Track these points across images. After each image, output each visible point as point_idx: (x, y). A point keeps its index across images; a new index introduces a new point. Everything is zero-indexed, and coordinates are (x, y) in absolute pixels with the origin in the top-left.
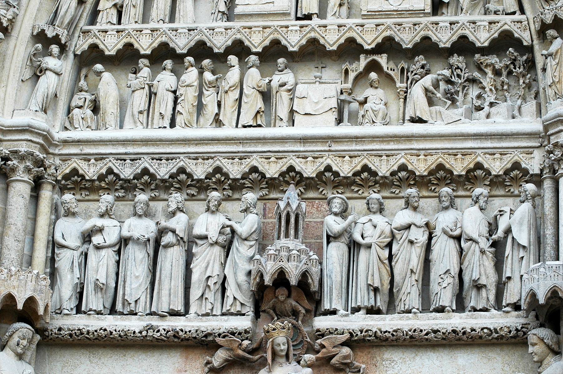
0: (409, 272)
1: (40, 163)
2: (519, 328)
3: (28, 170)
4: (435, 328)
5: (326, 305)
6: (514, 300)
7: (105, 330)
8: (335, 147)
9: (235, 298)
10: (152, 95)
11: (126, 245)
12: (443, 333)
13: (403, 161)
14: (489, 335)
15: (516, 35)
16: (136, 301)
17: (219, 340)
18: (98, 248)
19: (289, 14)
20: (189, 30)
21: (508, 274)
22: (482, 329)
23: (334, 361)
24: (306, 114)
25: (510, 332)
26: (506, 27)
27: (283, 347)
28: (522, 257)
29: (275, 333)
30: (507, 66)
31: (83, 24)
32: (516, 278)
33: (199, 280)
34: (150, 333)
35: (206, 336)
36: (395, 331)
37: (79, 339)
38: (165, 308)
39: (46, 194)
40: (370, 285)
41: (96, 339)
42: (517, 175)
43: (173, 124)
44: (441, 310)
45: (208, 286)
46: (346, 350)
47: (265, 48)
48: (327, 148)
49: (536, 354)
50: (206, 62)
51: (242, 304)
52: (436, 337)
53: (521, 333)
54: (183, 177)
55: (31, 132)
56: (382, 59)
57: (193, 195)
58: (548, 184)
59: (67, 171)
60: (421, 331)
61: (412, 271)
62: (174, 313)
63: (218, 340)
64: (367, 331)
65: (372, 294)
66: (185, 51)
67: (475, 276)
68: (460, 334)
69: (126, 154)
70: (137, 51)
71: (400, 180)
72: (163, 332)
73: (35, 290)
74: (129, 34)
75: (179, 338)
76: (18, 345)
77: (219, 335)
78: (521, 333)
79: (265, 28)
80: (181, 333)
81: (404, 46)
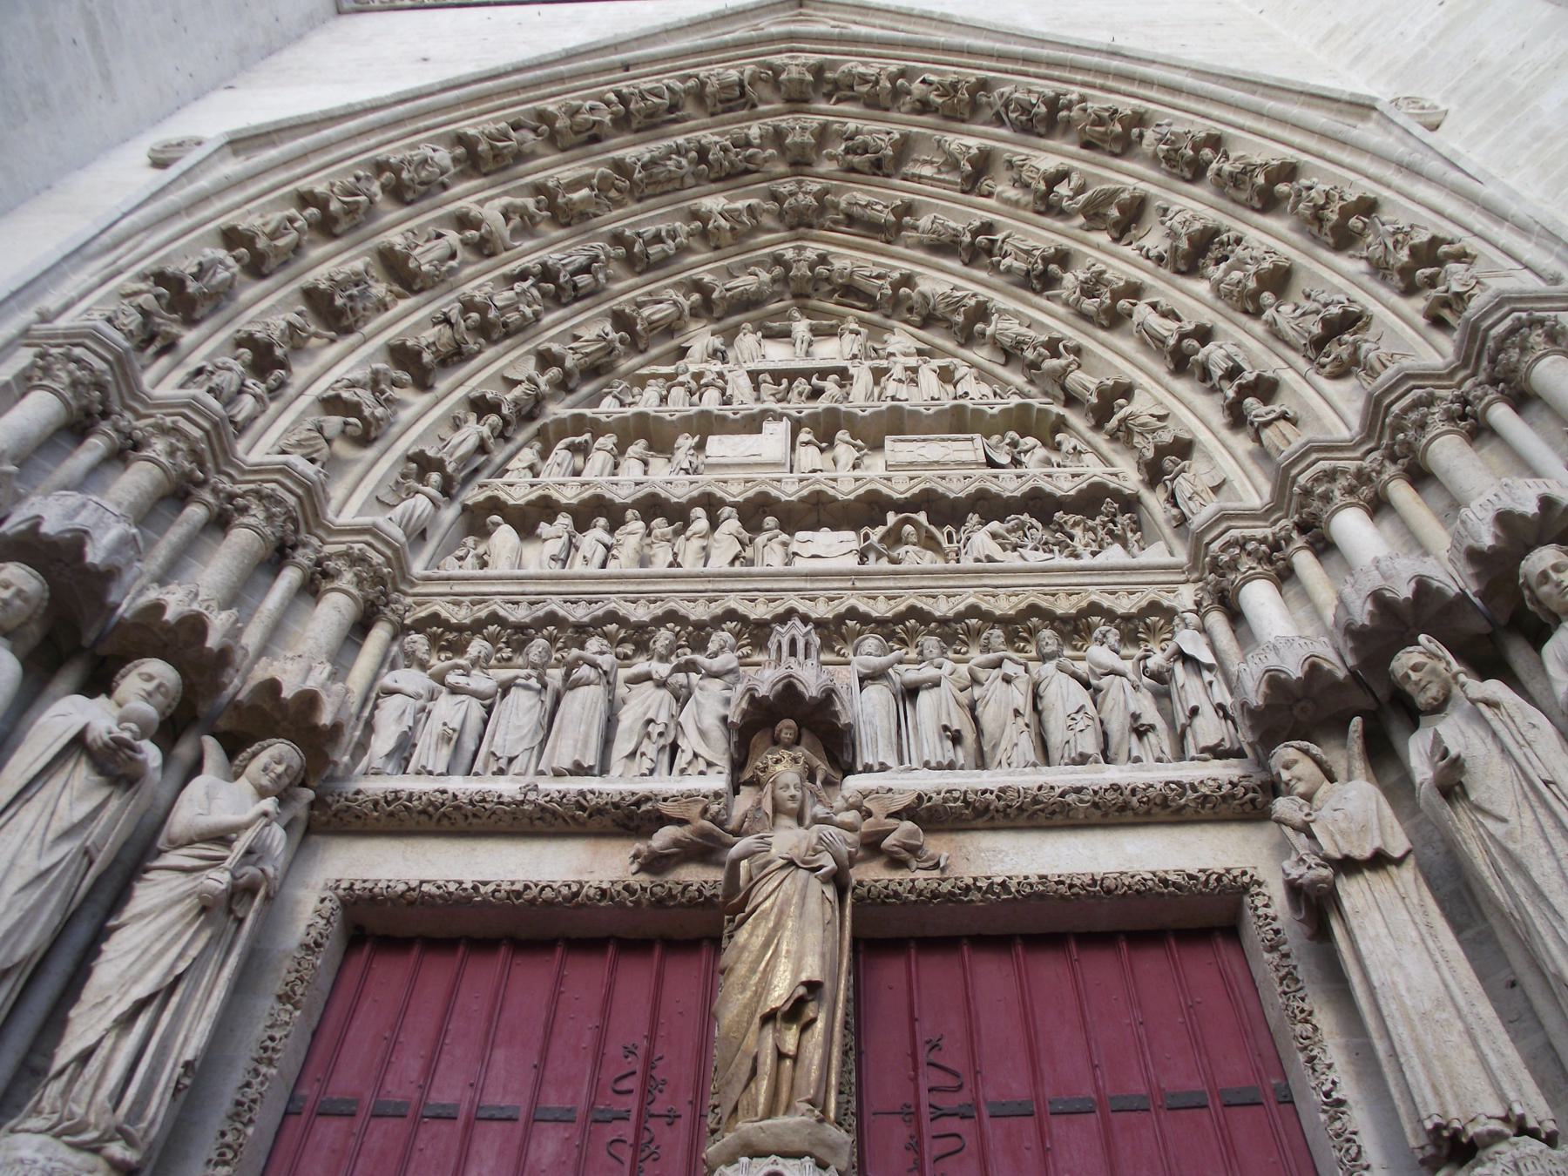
0: (1011, 713)
1: (379, 579)
2: (1235, 780)
3: (360, 582)
4: (1079, 785)
5: (869, 759)
6: (1211, 741)
7: (444, 792)
8: (858, 584)
9: (696, 755)
10: (571, 546)
11: (504, 695)
12: (1095, 792)
13: (972, 600)
14: (1181, 796)
15: (1112, 485)
16: (511, 760)
17: (668, 809)
18: (455, 690)
19: (784, 465)
20: (637, 484)
21: (1193, 703)
22: (1167, 783)
23: (888, 842)
24: (813, 557)
25: (1219, 788)
26: (1095, 479)
27: (793, 791)
28: (1211, 683)
29: (779, 768)
30: (1104, 525)
31: (481, 479)
32: (1207, 710)
33: (631, 729)
34: (532, 796)
35: (638, 803)
36: (1003, 790)
37: (391, 814)
38: (567, 763)
39: (379, 634)
40: (946, 728)
41: (424, 812)
42: (1155, 624)
43: (604, 565)
44: (1083, 759)
45: (648, 735)
46: (908, 825)
47: (747, 500)
48: (849, 585)
49: (1299, 779)
50: (659, 521)
51: (710, 764)
52: (1081, 801)
53: (1240, 791)
54: (613, 627)
55: (375, 535)
56: (922, 517)
57: (626, 657)
58: (1217, 621)
59: (423, 614)
60: (1052, 788)
61: (1017, 713)
62: (579, 770)
63: (661, 806)
64: (949, 791)
65: (949, 744)
66: (629, 501)
67: (1133, 708)
68: (1127, 792)
69: (523, 594)
70: (557, 502)
71: (968, 632)
72: (556, 795)
73: (323, 686)
74: (546, 487)
75: (583, 808)
76: (265, 769)
77: (665, 800)
78: (1240, 791)
79: (747, 481)
80: (589, 796)
81: (952, 496)
